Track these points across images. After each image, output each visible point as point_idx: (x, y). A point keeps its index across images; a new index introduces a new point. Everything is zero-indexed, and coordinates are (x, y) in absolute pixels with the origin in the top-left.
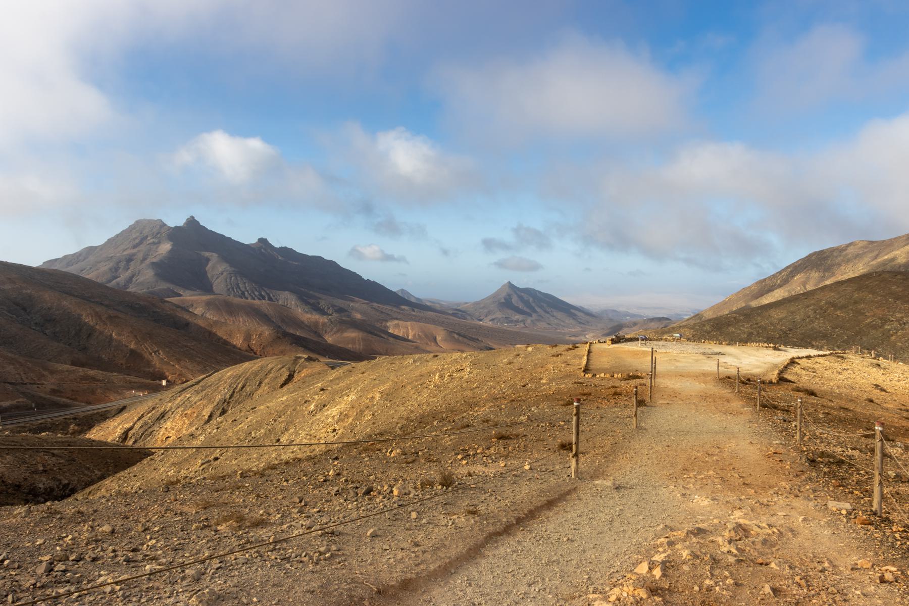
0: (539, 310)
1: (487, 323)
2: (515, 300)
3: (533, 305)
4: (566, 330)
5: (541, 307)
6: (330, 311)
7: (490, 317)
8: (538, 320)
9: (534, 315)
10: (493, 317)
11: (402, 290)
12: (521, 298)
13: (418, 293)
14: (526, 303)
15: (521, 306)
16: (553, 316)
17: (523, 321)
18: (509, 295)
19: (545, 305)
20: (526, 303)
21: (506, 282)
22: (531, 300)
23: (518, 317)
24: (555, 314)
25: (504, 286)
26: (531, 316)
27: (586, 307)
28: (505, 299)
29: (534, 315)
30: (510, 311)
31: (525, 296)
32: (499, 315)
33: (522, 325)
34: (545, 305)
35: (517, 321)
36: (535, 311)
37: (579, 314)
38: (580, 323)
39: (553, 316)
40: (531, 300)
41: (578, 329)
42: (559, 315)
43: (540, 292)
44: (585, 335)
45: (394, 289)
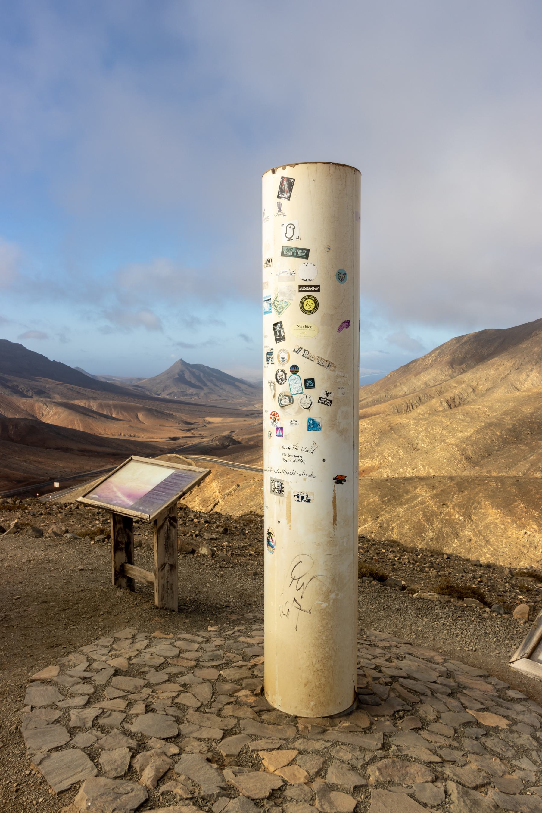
0: (209, 383)
1: (164, 395)
2: (187, 376)
3: (204, 379)
4: (235, 401)
5: (211, 381)
6: (30, 394)
7: (167, 392)
8: (210, 393)
9: (205, 388)
10: (170, 391)
11: (77, 368)
12: (192, 373)
13: (91, 369)
14: (198, 378)
15: (193, 381)
16: (222, 389)
17: (197, 395)
18: (182, 371)
19: (214, 379)
20: (198, 378)
21: (178, 359)
22: (202, 375)
23: (192, 391)
24: (223, 387)
25: (177, 362)
26: (202, 389)
27: (244, 379)
28: (179, 375)
29: (205, 388)
30: (184, 387)
31: (196, 372)
32: (174, 389)
33: (196, 398)
34: (214, 379)
35: (192, 395)
36: (206, 385)
37: (243, 386)
38: (246, 394)
39: (222, 389)
40: (202, 375)
41: (244, 400)
42: (227, 387)
43: (208, 367)
44: (253, 405)
45: (73, 366)
